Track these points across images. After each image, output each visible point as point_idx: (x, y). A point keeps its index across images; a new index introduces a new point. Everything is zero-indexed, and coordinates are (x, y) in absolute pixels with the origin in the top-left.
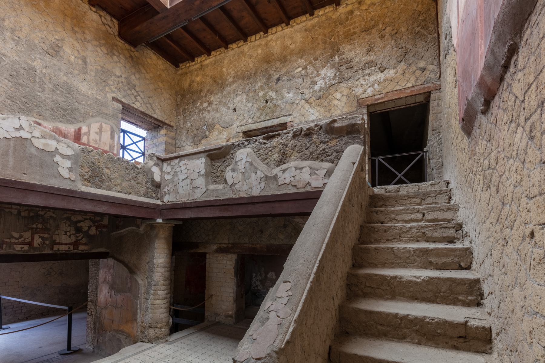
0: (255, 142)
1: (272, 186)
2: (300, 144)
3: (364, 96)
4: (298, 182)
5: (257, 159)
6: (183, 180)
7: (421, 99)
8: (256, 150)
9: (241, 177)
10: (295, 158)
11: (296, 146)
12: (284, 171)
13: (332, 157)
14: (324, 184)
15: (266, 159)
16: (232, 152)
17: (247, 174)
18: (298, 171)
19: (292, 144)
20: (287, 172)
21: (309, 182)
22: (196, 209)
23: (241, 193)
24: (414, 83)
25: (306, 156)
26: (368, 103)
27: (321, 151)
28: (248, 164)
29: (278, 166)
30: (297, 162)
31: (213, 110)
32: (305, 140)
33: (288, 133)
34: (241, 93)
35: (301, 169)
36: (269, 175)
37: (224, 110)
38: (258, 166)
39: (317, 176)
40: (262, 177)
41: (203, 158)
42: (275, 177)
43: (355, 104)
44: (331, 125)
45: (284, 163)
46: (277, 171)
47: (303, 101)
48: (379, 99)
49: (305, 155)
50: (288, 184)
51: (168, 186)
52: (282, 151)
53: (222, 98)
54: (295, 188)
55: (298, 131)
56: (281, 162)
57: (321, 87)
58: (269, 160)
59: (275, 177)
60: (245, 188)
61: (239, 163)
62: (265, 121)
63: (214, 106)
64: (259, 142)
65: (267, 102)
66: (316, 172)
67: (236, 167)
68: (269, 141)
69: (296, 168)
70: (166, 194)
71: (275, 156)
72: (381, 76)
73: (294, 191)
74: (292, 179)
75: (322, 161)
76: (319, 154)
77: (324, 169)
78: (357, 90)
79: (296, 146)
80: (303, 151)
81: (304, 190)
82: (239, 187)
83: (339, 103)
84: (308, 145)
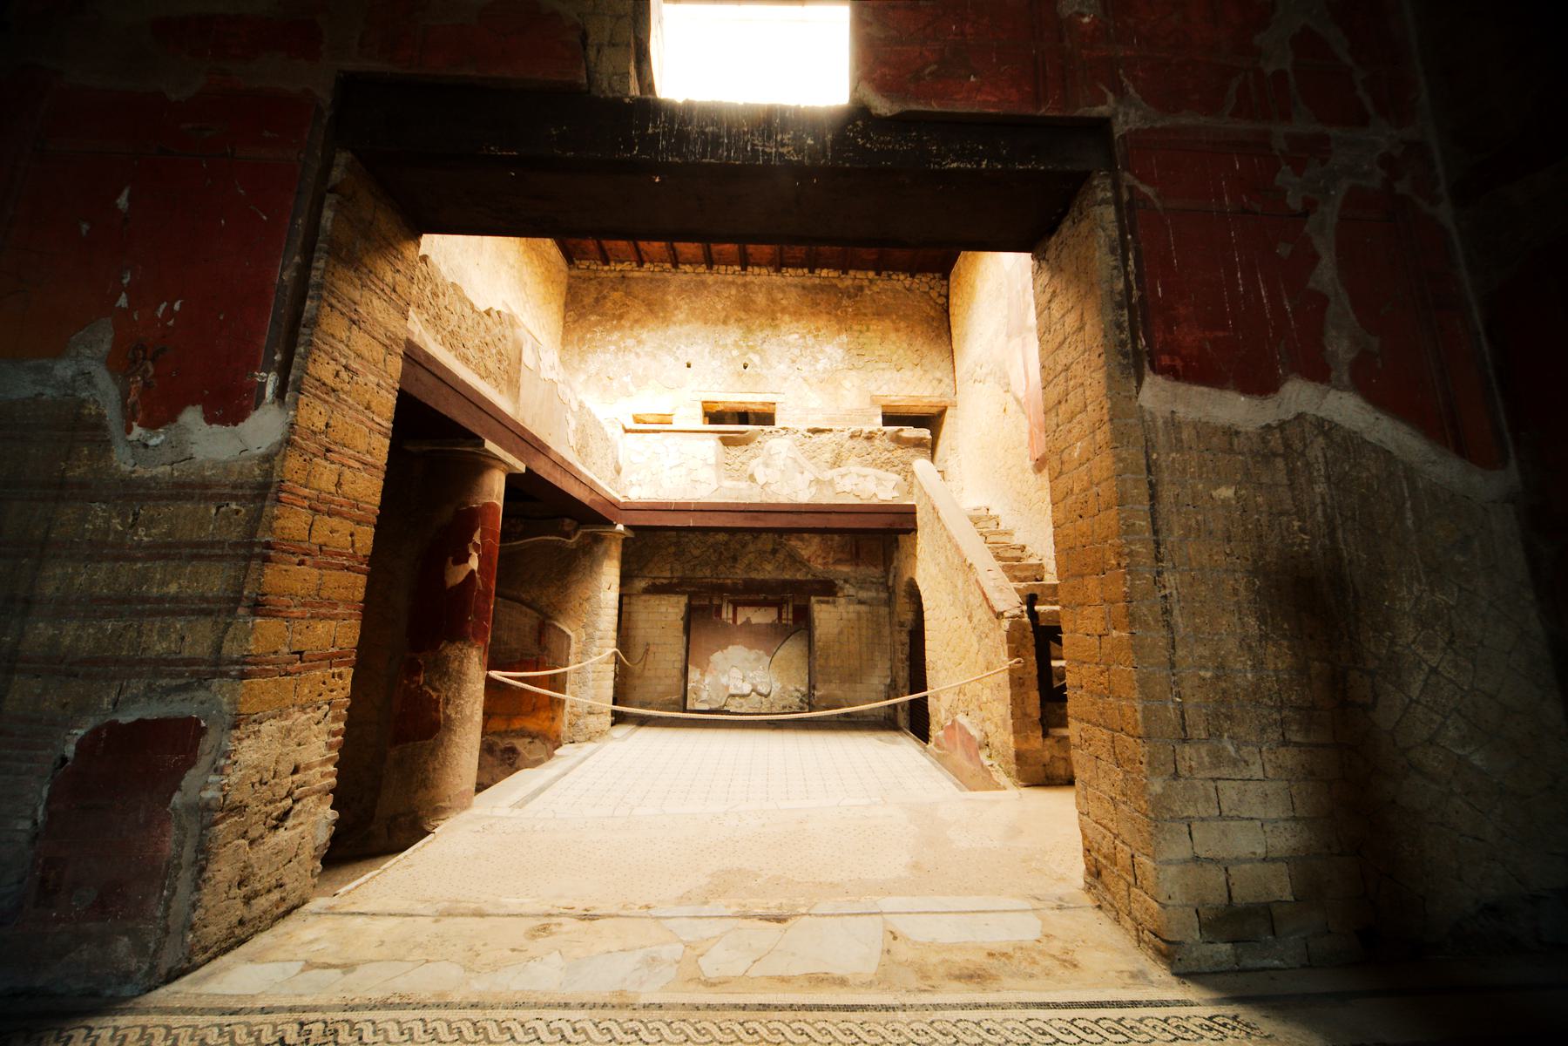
3: (878, 393)
6: (671, 468)
7: (934, 411)
8: (798, 444)
12: (843, 476)
18: (862, 479)
20: (846, 477)
22: (699, 514)
26: (884, 403)
28: (789, 461)
29: (831, 468)
32: (865, 442)
34: (700, 342)
41: (712, 441)
42: (831, 482)
47: (800, 380)
48: (894, 401)
51: (638, 474)
53: (665, 340)
63: (646, 349)
65: (745, 368)
68: (816, 435)
69: (859, 475)
70: (632, 484)
74: (854, 487)
84: (870, 450)
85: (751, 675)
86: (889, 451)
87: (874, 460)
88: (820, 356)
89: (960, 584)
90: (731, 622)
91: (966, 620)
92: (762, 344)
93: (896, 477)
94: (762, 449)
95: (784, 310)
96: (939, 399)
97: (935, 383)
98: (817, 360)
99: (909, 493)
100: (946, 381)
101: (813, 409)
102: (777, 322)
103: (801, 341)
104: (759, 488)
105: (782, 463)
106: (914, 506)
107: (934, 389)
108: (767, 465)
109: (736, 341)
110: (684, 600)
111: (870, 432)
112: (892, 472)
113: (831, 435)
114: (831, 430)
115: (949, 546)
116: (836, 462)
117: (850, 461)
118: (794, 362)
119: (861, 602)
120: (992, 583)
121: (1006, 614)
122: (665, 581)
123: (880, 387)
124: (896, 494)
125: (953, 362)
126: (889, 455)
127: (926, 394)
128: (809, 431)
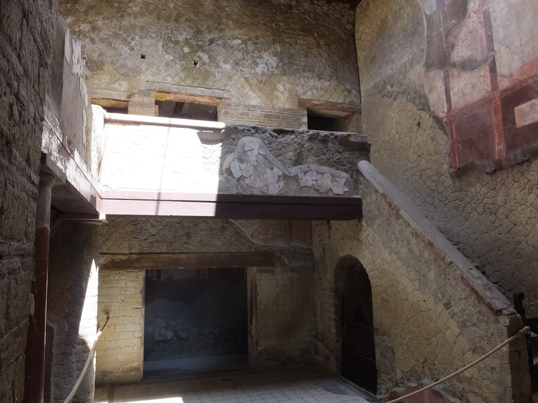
0: (264, 133)
1: (291, 186)
2: (316, 148)
3: (304, 97)
4: (320, 186)
5: (269, 153)
8: (267, 142)
9: (252, 171)
10: (313, 161)
11: (312, 149)
12: (305, 173)
13: (346, 167)
14: (344, 192)
15: (280, 155)
16: (234, 137)
17: (260, 169)
18: (320, 175)
19: (309, 146)
21: (331, 188)
23: (253, 189)
24: (343, 100)
25: (323, 161)
27: (337, 160)
28: (261, 157)
29: (295, 165)
30: (315, 165)
31: (102, 40)
32: (321, 145)
33: (303, 133)
34: (154, 36)
35: (323, 174)
36: (286, 173)
37: (125, 50)
38: (274, 162)
39: (338, 184)
40: (280, 175)
42: (296, 178)
43: (297, 103)
44: (347, 138)
45: (301, 164)
46: (294, 171)
47: (243, 80)
49: (322, 160)
50: (310, 188)
52: (298, 151)
53: (120, 29)
54: (317, 192)
55: (315, 135)
56: (297, 161)
57: (263, 72)
58: (283, 157)
59: (296, 178)
60: (259, 184)
61: (249, 153)
62: (192, 87)
64: (270, 134)
66: (337, 179)
67: (243, 157)
68: (281, 136)
69: (318, 173)
71: (291, 154)
72: (318, 84)
73: (317, 195)
74: (314, 183)
75: (338, 169)
76: (335, 162)
77: (344, 178)
78: (298, 88)
79: (312, 149)
80: (320, 156)
81: (327, 196)
82: (250, 182)
83: (282, 96)
84: (324, 151)
85: (173, 323)
86: (340, 153)
87: (328, 159)
88: (259, 61)
89: (431, 275)
90: (155, 279)
91: (441, 306)
92: (210, 44)
93: (345, 175)
94: (236, 146)
95: (228, 16)
96: (349, 106)
97: (346, 93)
98: (257, 64)
99: (356, 188)
100: (354, 92)
101: (254, 106)
102: (223, 27)
103: (243, 46)
104: (235, 181)
105: (255, 159)
106: (359, 200)
107: (346, 98)
108: (241, 161)
109: (186, 39)
110: (141, 275)
111: (325, 136)
112: (342, 170)
113: (293, 136)
114: (293, 132)
115: (413, 241)
116: (298, 160)
117: (309, 160)
118: (237, 64)
119: (293, 270)
120: (480, 283)
121: (504, 312)
122: (124, 258)
123: (306, 92)
124: (346, 189)
125: (359, 78)
126: (339, 156)
127: (340, 101)
128: (275, 131)
